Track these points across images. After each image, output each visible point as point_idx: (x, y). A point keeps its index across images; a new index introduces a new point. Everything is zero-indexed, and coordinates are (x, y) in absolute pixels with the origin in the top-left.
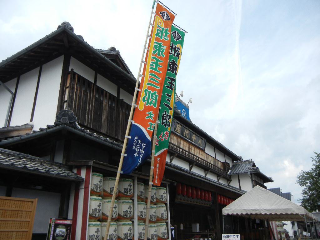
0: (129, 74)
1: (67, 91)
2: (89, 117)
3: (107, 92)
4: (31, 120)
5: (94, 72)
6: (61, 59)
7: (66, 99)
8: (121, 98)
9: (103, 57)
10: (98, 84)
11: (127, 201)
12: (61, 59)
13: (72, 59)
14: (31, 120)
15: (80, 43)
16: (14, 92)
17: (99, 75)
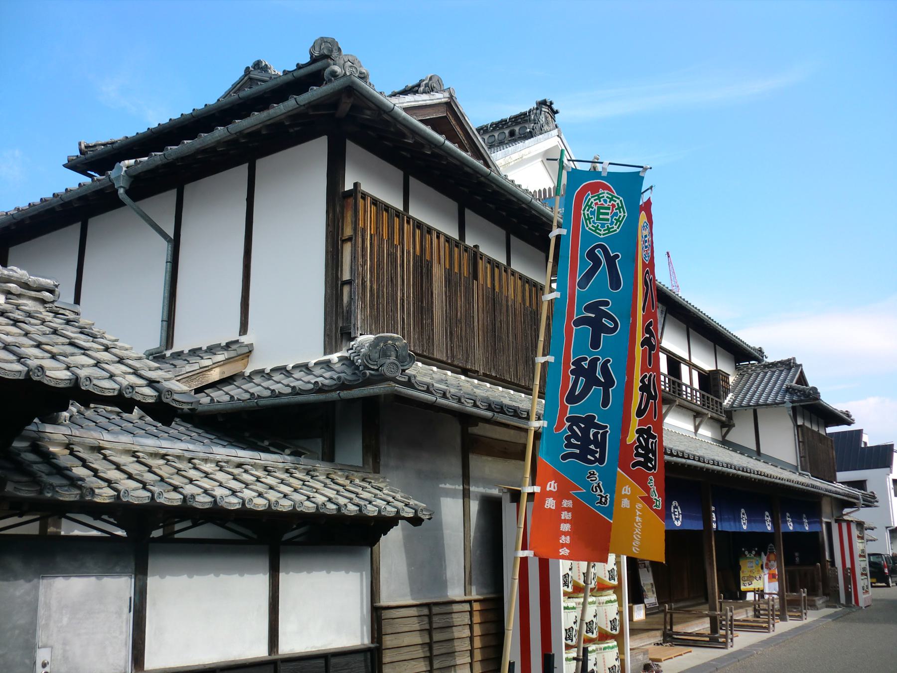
0: (488, 166)
1: (347, 249)
2: (403, 319)
3: (439, 234)
4: (244, 329)
5: (399, 174)
6: (319, 147)
7: (346, 276)
8: (470, 242)
9: (439, 142)
10: (412, 213)
11: (611, 645)
12: (319, 147)
13: (352, 148)
14: (244, 329)
15: (385, 112)
16: (171, 233)
17: (413, 181)
